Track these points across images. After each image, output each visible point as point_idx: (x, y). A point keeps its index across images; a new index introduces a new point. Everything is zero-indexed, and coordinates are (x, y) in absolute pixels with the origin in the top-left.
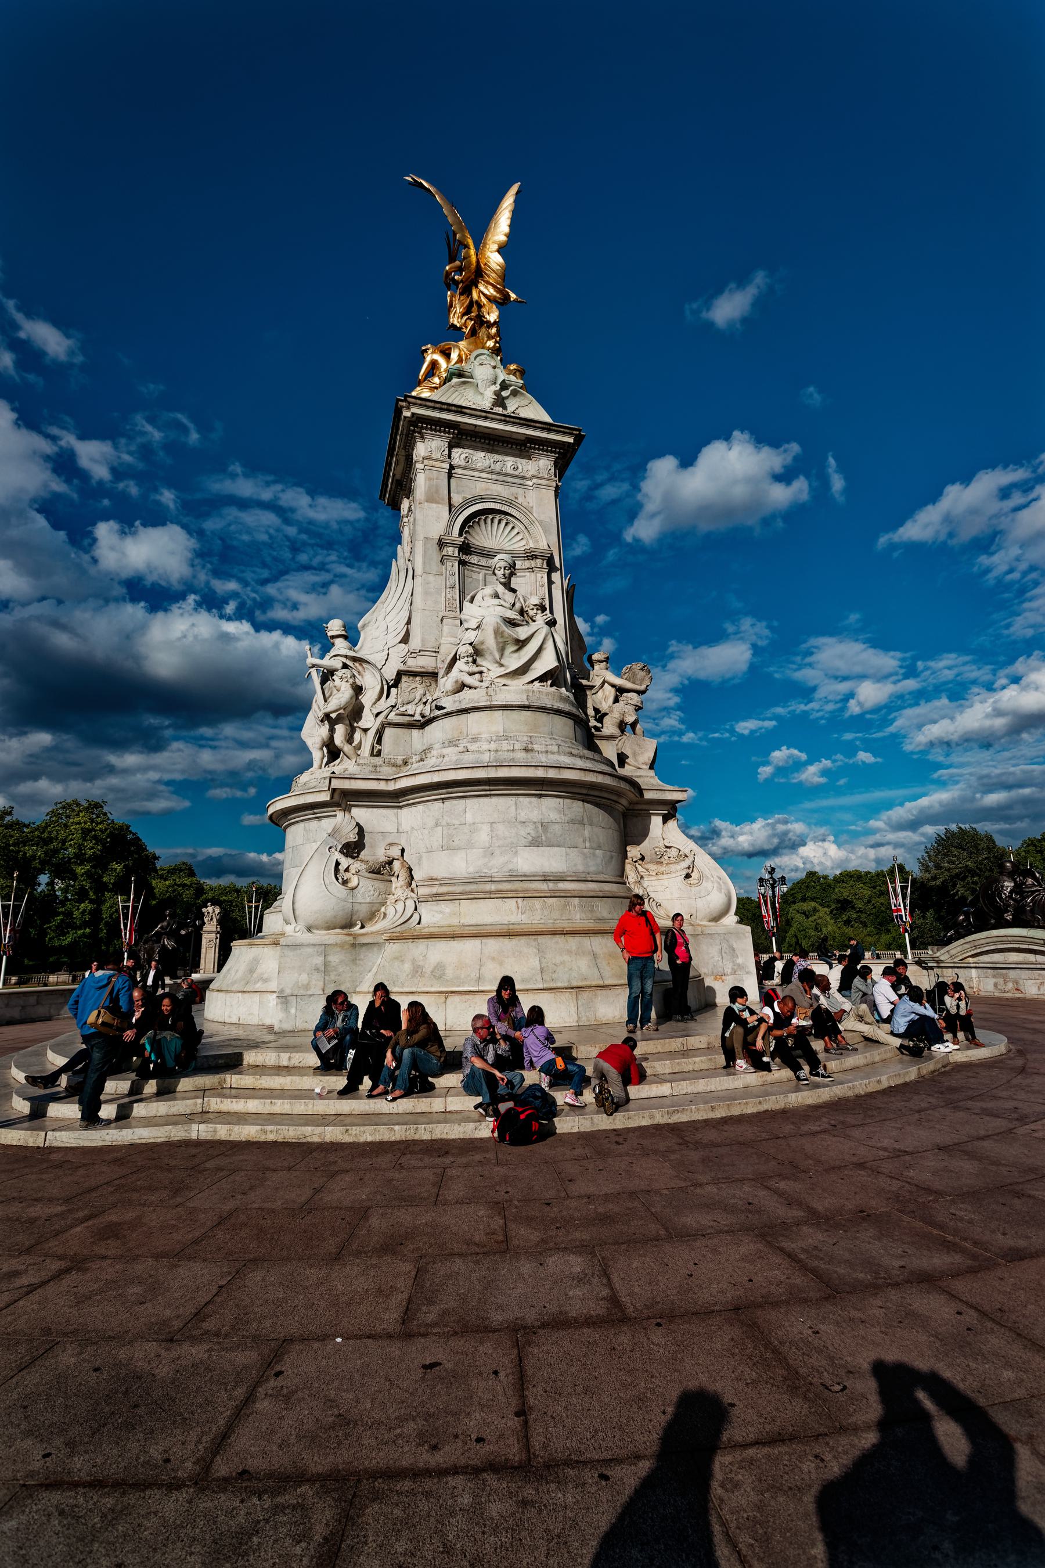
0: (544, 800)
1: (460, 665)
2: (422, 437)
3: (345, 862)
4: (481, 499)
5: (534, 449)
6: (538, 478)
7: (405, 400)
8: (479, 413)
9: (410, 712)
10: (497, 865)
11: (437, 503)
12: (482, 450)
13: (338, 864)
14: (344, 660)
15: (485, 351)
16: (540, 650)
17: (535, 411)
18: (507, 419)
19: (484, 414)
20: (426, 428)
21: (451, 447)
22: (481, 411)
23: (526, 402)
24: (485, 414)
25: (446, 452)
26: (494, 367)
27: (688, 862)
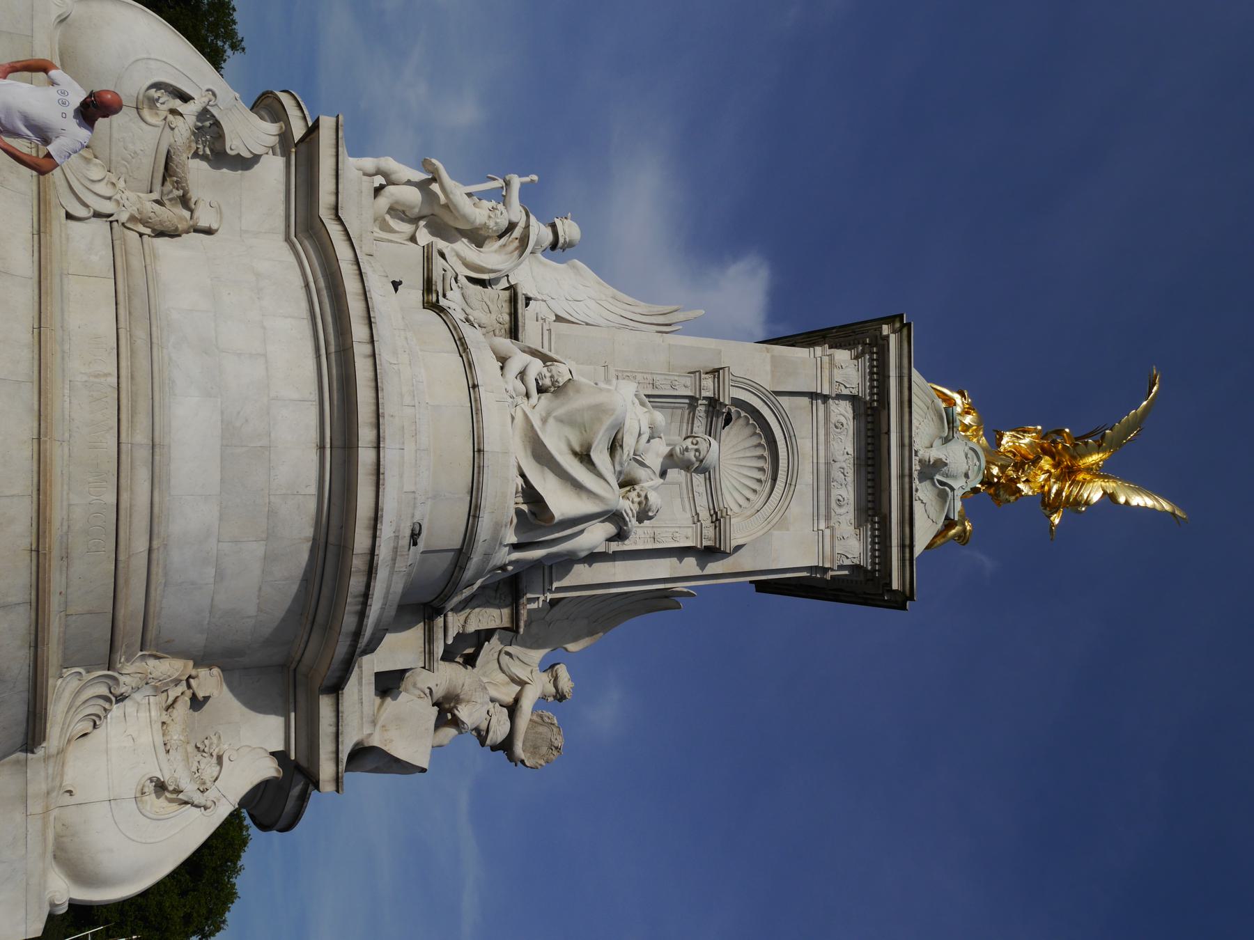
0: (314, 456)
1: (536, 366)
2: (856, 358)
3: (190, 109)
4: (789, 437)
5: (873, 529)
6: (832, 536)
7: (903, 325)
8: (906, 434)
9: (449, 294)
10: (183, 364)
11: (772, 372)
12: (858, 449)
13: (185, 98)
14: (522, 224)
15: (983, 464)
16: (577, 486)
17: (923, 535)
18: (906, 476)
19: (906, 441)
20: (871, 360)
21: (853, 399)
22: (910, 437)
23: (933, 514)
24: (907, 445)
25: (846, 392)
26: (967, 476)
27: (190, 789)
